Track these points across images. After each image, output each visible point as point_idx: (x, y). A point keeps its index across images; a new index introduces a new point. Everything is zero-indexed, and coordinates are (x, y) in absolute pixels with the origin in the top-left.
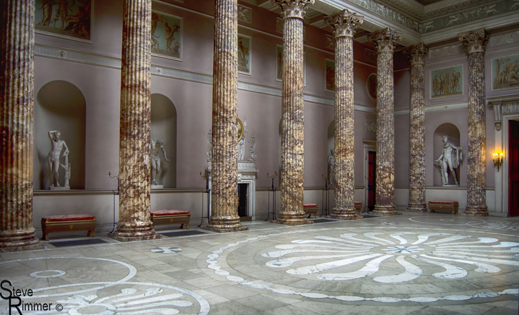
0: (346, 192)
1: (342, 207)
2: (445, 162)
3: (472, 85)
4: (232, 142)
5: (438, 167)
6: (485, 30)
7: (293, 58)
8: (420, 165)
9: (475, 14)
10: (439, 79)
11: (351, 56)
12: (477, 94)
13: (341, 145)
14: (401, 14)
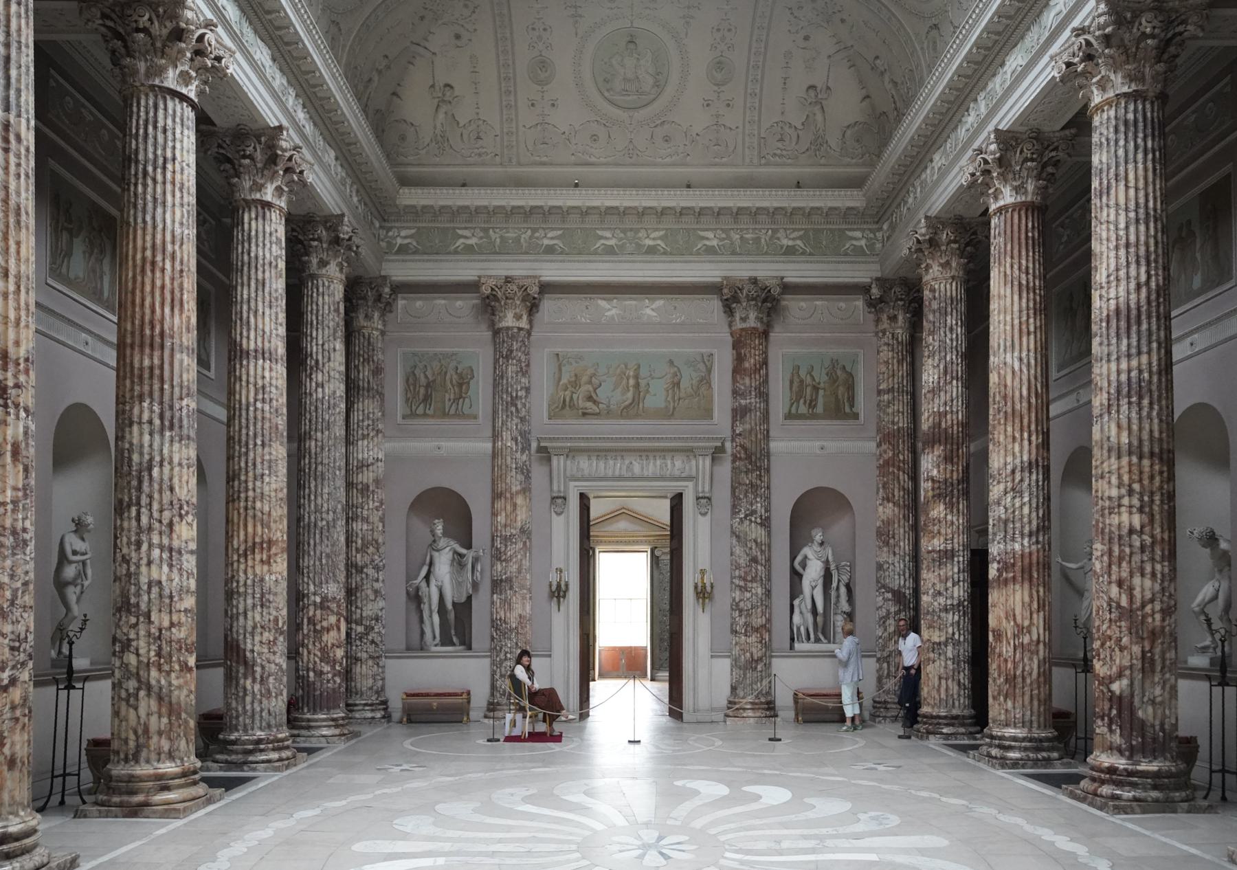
0: (271, 680)
1: (261, 729)
2: (437, 586)
3: (507, 403)
4: (25, 488)
5: (415, 598)
6: (539, 282)
7: (173, 221)
8: (376, 592)
9: (517, 240)
10: (422, 375)
11: (282, 265)
12: (517, 425)
13: (255, 526)
14: (358, 191)
